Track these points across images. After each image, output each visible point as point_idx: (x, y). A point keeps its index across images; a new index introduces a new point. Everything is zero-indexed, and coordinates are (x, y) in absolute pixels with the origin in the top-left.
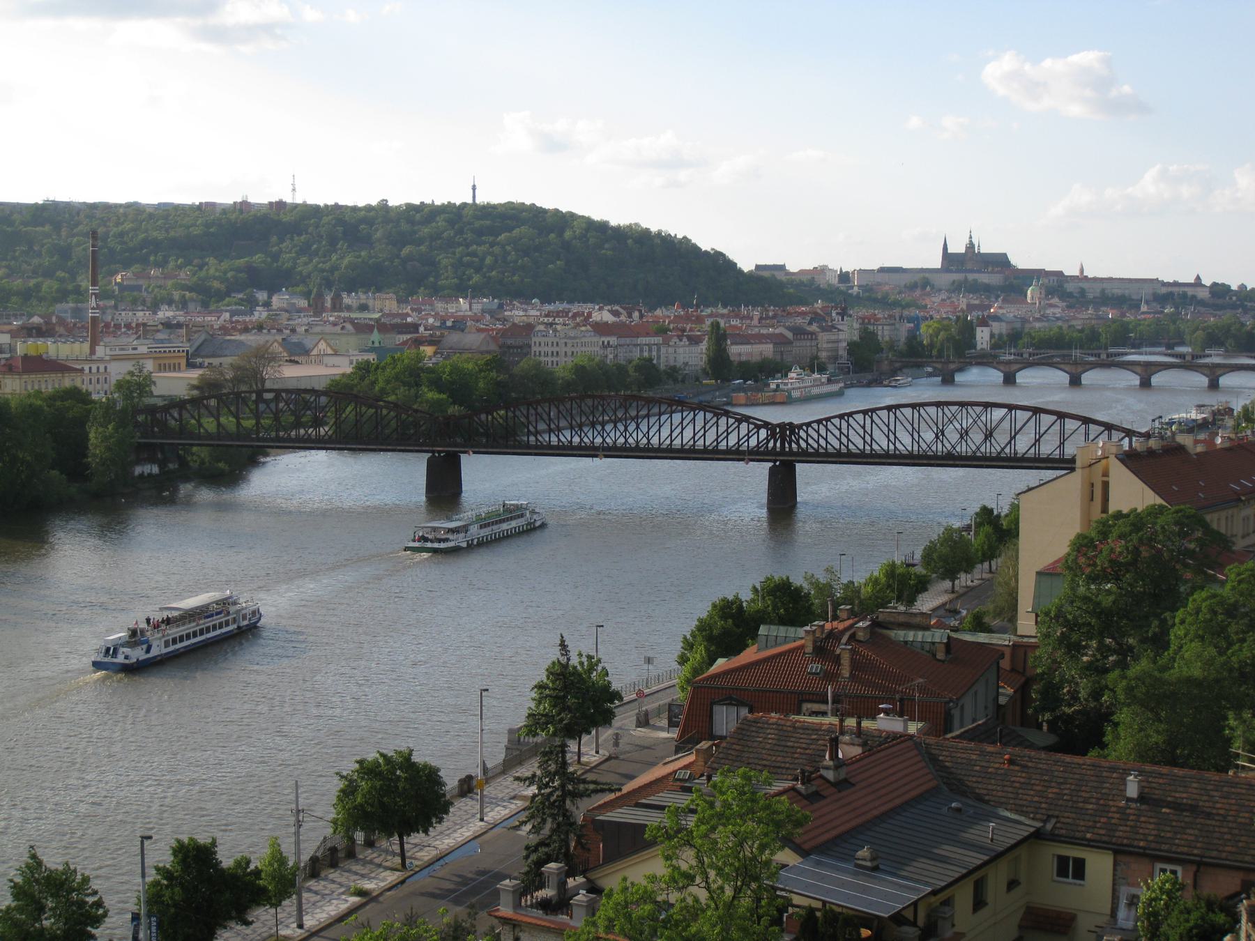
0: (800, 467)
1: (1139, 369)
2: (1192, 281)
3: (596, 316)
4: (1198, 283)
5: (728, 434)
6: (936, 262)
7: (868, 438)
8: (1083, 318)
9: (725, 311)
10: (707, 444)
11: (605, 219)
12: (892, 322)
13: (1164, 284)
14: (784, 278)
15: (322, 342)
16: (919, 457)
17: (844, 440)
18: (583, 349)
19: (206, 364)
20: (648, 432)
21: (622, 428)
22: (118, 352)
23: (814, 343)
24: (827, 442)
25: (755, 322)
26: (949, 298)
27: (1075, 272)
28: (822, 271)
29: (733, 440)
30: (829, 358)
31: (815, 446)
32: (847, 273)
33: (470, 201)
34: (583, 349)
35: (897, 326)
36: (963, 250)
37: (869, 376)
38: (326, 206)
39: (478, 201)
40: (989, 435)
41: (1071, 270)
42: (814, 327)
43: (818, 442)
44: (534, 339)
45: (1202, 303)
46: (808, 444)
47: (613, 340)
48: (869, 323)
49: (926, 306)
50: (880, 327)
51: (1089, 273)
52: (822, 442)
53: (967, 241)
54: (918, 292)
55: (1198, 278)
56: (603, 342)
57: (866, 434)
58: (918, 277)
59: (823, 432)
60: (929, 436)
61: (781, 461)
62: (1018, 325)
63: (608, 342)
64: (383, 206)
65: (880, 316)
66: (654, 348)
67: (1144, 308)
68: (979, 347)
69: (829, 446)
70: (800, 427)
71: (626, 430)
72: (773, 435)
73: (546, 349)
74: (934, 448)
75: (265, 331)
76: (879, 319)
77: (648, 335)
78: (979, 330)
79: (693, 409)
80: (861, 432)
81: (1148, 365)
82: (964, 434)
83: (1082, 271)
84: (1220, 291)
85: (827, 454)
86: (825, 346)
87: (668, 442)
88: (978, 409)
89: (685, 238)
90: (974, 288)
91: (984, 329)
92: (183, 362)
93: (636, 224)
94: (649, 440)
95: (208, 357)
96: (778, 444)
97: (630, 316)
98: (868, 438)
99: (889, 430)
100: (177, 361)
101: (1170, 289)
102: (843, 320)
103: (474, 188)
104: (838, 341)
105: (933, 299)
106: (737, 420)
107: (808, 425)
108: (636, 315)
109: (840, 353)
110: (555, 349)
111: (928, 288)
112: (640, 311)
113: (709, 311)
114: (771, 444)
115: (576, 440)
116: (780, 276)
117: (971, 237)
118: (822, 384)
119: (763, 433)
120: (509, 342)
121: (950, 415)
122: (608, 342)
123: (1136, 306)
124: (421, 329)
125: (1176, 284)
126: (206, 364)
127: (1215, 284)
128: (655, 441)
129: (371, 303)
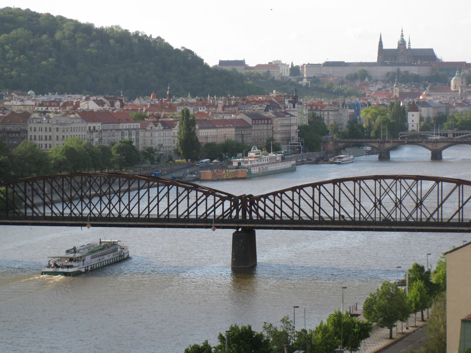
3: (84, 106)
5: (197, 205)
6: (373, 57)
7: (316, 208)
9: (194, 100)
10: (180, 213)
11: (90, 21)
12: (337, 108)
14: (243, 72)
16: (360, 223)
17: (296, 209)
18: (73, 134)
20: (129, 204)
21: (106, 201)
23: (270, 127)
24: (282, 211)
25: (220, 109)
28: (275, 65)
29: (201, 210)
30: (283, 139)
31: (272, 214)
32: (297, 67)
34: (73, 134)
35: (341, 111)
36: (395, 46)
40: (419, 204)
42: (270, 114)
43: (274, 211)
44: (30, 125)
46: (266, 213)
47: (98, 126)
48: (317, 109)
49: (364, 95)
50: (326, 113)
52: (278, 211)
53: (399, 38)
54: (358, 83)
56: (90, 128)
57: (315, 204)
58: (358, 70)
59: (278, 202)
60: (368, 204)
61: (243, 228)
62: (443, 110)
63: (94, 127)
65: (326, 103)
66: (134, 132)
68: (410, 128)
69: (283, 215)
70: (259, 198)
71: (110, 202)
72: (235, 206)
73: (40, 133)
74: (373, 216)
77: (128, 121)
78: (410, 114)
79: (167, 185)
80: (311, 202)
82: (398, 203)
85: (282, 221)
86: (279, 129)
87: (146, 212)
88: (410, 182)
89: (159, 38)
91: (416, 114)
93: (117, 27)
94: (130, 211)
96: (240, 214)
97: (112, 105)
98: (316, 208)
99: (334, 200)
102: (294, 107)
104: (290, 125)
105: (371, 89)
106: (205, 193)
107: (266, 196)
108: (118, 104)
109: (292, 135)
110: (48, 134)
111: (367, 80)
112: (121, 101)
113: (180, 100)
114: (234, 214)
115: (67, 211)
116: (240, 70)
117: (402, 36)
118: (277, 162)
119: (227, 204)
120: (8, 128)
121: (386, 187)
122: (94, 127)
128: (135, 212)
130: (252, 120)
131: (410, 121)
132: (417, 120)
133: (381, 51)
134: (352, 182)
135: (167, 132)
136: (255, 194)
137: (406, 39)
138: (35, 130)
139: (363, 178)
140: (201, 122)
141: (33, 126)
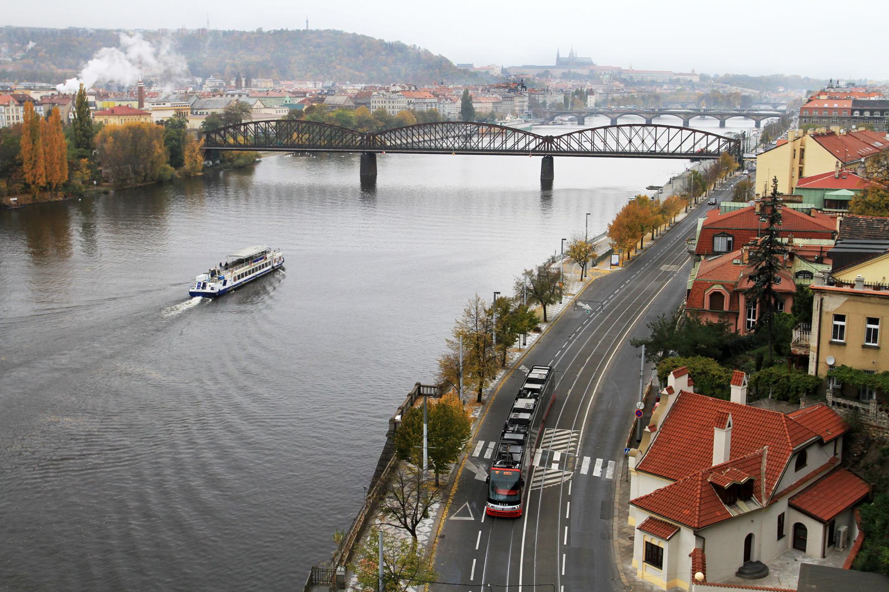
1: (682, 116)
4: (693, 74)
6: (553, 63)
11: (382, 38)
13: (675, 74)
18: (398, 105)
19: (199, 113)
22: (155, 106)
27: (628, 68)
30: (519, 110)
33: (305, 28)
34: (398, 105)
37: (541, 120)
38: (229, 31)
39: (309, 29)
44: (372, 100)
50: (537, 95)
54: (544, 79)
55: (693, 71)
58: (542, 71)
66: (434, 104)
67: (665, 87)
68: (588, 106)
75: (224, 96)
76: (537, 91)
78: (589, 97)
86: (517, 104)
92: (189, 112)
93: (398, 41)
100: (186, 111)
103: (307, 22)
104: (524, 102)
105: (552, 82)
110: (384, 105)
116: (471, 70)
117: (572, 49)
118: (522, 123)
123: (661, 85)
124: (308, 95)
126: (199, 113)
127: (702, 74)
129: (259, 84)
133: (558, 59)
134: (603, 129)
135: (453, 105)
136: (554, 136)
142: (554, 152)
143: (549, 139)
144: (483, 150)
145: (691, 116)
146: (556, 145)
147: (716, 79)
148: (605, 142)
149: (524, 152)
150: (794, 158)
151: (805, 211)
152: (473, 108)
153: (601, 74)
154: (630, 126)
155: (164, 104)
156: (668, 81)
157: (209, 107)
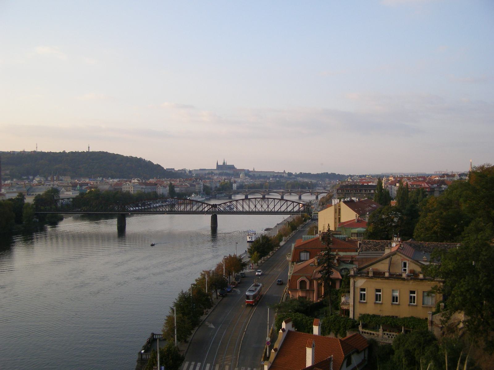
0: (219, 216)
1: (281, 193)
2: (283, 172)
6: (215, 168)
8: (258, 182)
12: (210, 182)
15: (63, 188)
19: (31, 194)
24: (220, 209)
25: (178, 182)
26: (219, 177)
28: (184, 170)
32: (191, 170)
33: (88, 151)
35: (212, 184)
41: (251, 169)
42: (195, 183)
45: (286, 178)
47: (144, 187)
50: (207, 184)
51: (256, 170)
54: (210, 176)
62: (242, 184)
64: (64, 152)
65: (207, 181)
67: (271, 179)
70: (218, 205)
75: (45, 185)
78: (233, 184)
81: (283, 192)
83: (254, 170)
84: (290, 174)
90: (227, 174)
91: (235, 184)
95: (31, 192)
101: (277, 174)
103: (89, 147)
104: (200, 187)
105: (215, 177)
109: (201, 190)
111: (213, 174)
112: (145, 180)
113: (164, 180)
116: (173, 171)
120: (116, 187)
124: (89, 185)
125: (278, 173)
126: (31, 194)
129: (63, 179)
130: (190, 185)
131: (233, 187)
132: (236, 186)
134: (242, 200)
137: (225, 162)
138: (124, 188)
139: (226, 203)
140: (176, 185)
141: (124, 187)
142: (217, 212)
143: (214, 206)
144: (181, 212)
145: (284, 193)
146: (218, 208)
147: (297, 176)
148: (243, 207)
149: (202, 213)
150: (336, 213)
151: (343, 238)
152: (175, 190)
153: (239, 173)
154: (255, 198)
155: (12, 190)
156: (272, 176)
157: (37, 191)
